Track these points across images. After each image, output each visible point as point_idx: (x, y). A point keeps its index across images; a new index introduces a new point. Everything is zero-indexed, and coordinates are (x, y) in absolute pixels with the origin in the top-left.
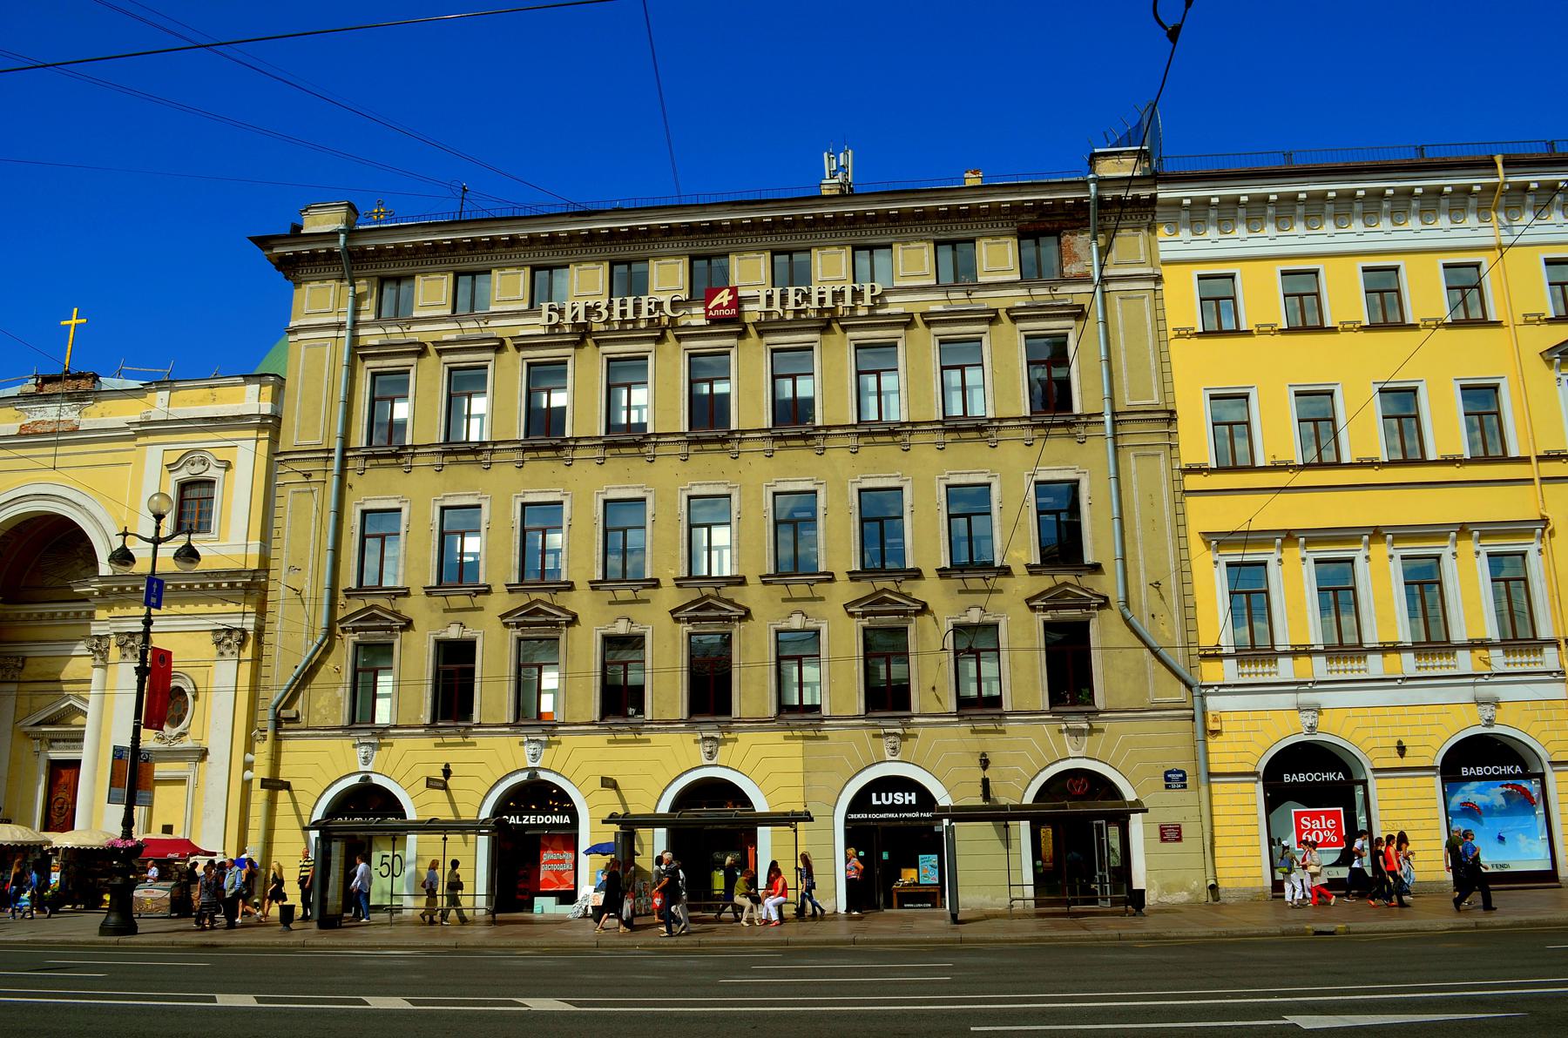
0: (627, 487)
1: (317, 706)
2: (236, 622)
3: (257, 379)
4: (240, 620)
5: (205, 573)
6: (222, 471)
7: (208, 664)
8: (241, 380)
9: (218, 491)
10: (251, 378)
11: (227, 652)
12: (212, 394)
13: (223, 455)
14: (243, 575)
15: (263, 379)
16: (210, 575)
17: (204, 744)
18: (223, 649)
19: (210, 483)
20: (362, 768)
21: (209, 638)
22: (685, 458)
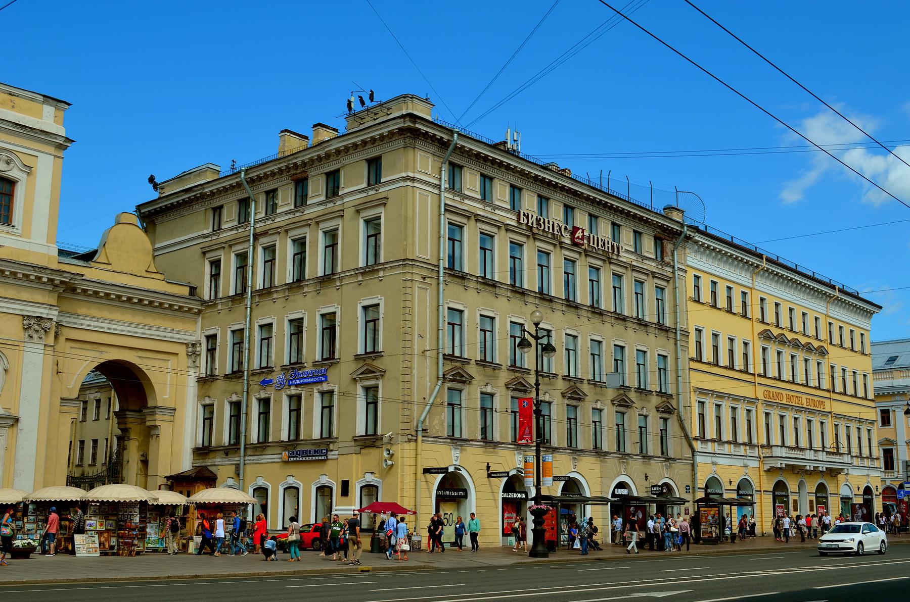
0: (546, 323)
1: (434, 424)
2: (43, 312)
3: (55, 103)
4: (46, 311)
5: (33, 267)
6: (25, 176)
7: (16, 343)
8: (41, 98)
9: (20, 193)
10: (50, 100)
11: (35, 336)
12: (11, 101)
13: (28, 161)
14: (65, 275)
15: (60, 104)
16: (37, 269)
17: (14, 413)
18: (31, 332)
19: (12, 183)
20: (455, 463)
21: (17, 323)
22: (564, 313)
